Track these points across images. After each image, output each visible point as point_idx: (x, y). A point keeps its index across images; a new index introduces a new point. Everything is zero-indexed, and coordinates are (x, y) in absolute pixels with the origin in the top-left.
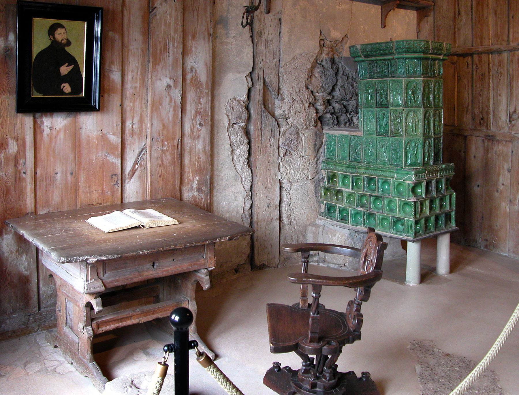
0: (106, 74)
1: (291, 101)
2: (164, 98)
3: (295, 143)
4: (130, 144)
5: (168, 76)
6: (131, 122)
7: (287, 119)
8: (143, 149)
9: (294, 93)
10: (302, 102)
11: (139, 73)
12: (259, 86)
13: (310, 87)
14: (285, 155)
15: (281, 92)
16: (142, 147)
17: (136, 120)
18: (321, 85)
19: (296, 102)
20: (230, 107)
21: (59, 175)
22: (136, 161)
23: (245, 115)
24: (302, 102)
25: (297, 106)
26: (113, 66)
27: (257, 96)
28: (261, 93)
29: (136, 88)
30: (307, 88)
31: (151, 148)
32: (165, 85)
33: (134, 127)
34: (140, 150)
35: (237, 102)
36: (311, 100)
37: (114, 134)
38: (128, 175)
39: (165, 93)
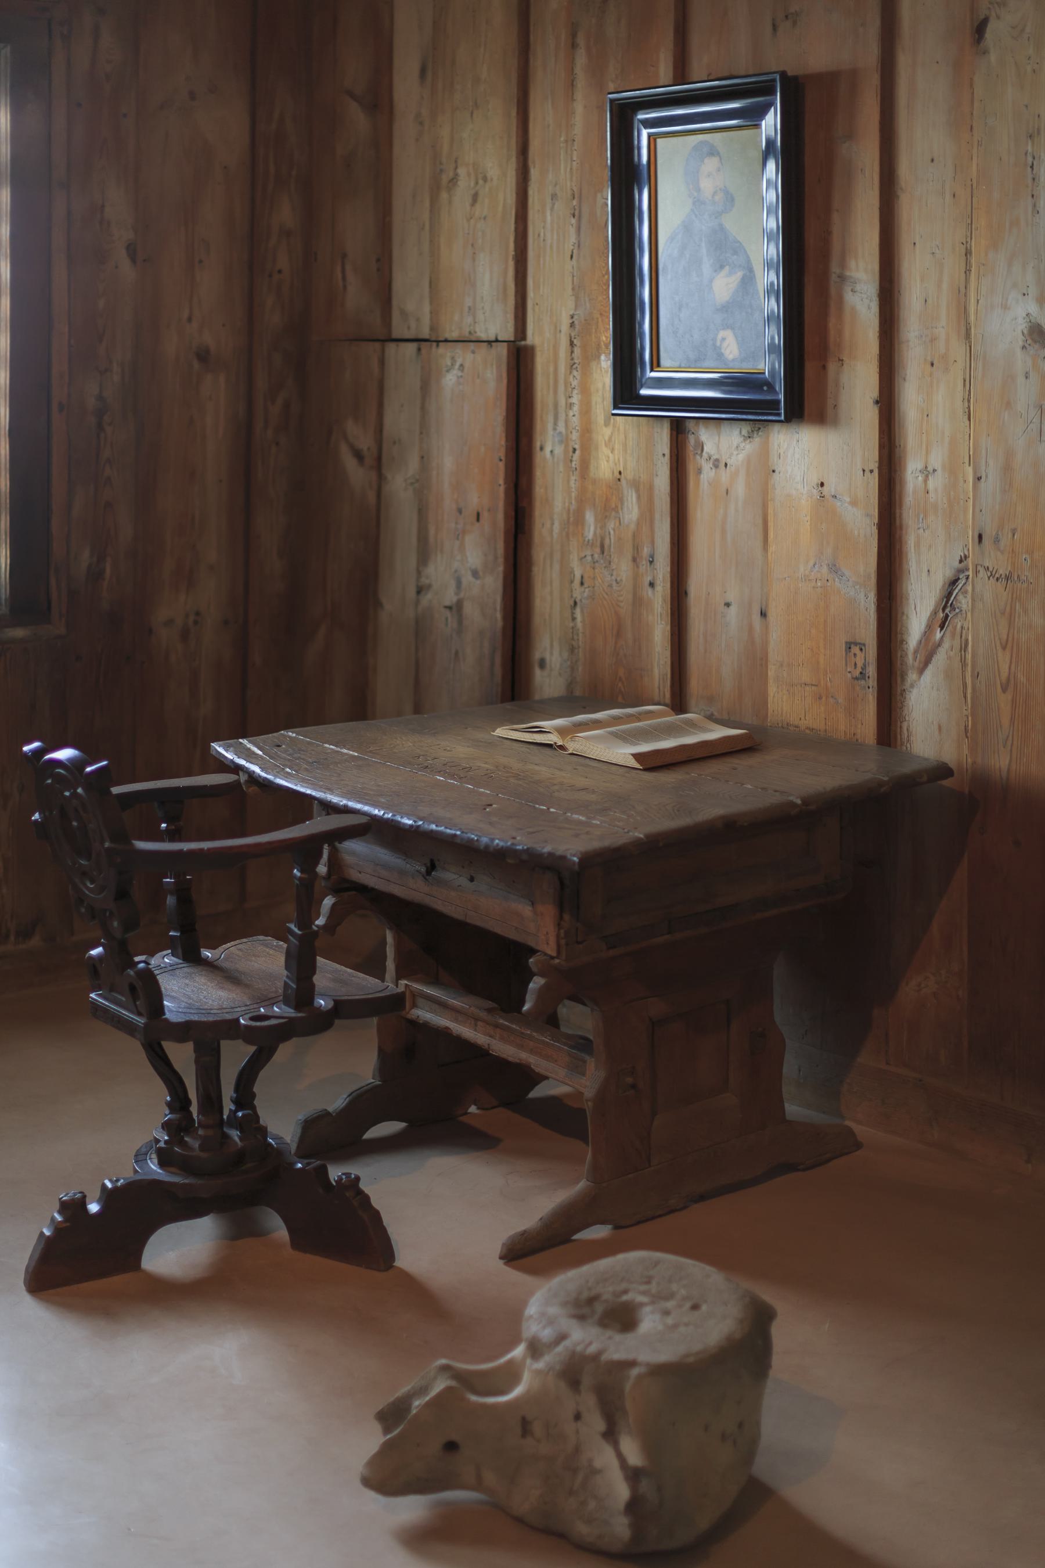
0: (833, 291)
2: (1020, 379)
4: (918, 545)
5: (1033, 291)
6: (920, 466)
8: (960, 571)
11: (945, 286)
16: (956, 564)
17: (937, 459)
21: (733, 609)
22: (935, 613)
26: (852, 264)
29: (933, 340)
31: (977, 572)
32: (1022, 326)
33: (931, 484)
34: (949, 574)
37: (854, 503)
38: (915, 659)
39: (1021, 361)
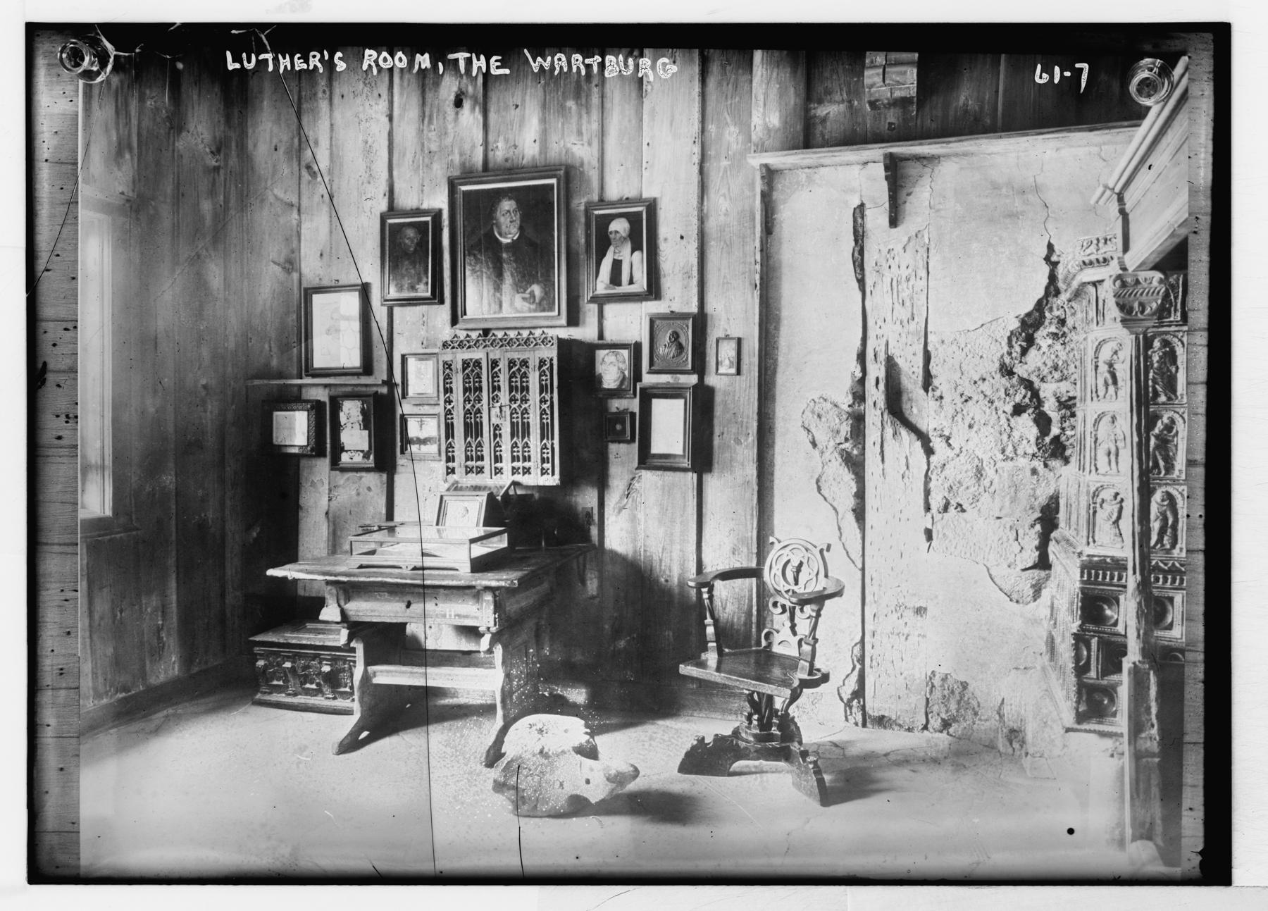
1: (959, 400)
3: (972, 489)
7: (948, 438)
9: (967, 383)
10: (992, 402)
12: (876, 371)
13: (1020, 370)
14: (946, 508)
15: (936, 382)
18: (1050, 364)
19: (970, 403)
20: (813, 412)
23: (846, 428)
24: (992, 402)
25: (976, 410)
27: (876, 395)
28: (882, 386)
30: (1007, 371)
35: (829, 406)
36: (1018, 399)
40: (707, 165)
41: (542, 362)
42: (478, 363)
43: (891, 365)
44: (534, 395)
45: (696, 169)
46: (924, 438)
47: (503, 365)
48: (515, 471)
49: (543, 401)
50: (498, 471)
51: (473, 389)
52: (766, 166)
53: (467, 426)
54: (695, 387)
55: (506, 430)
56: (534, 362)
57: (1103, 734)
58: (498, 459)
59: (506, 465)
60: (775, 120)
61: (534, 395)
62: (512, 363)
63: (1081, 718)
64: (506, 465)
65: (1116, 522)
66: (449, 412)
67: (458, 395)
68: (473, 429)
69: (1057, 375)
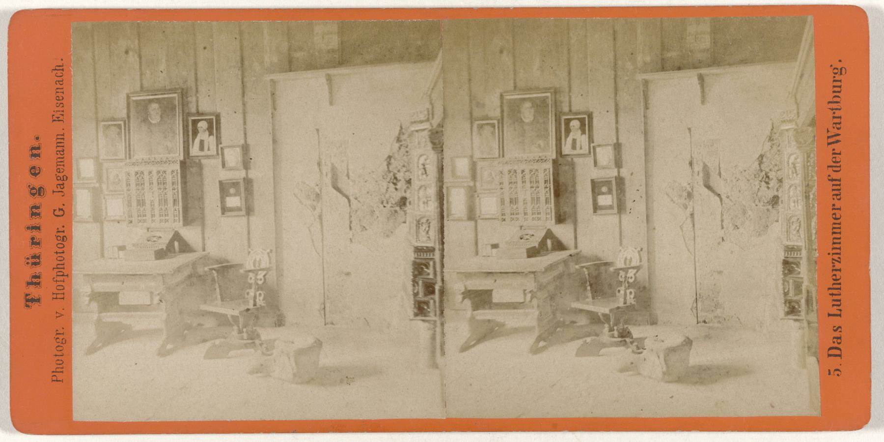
40: (245, 79)
41: (173, 172)
42: (142, 173)
43: (334, 169)
44: (169, 186)
45: (240, 82)
46: (347, 197)
47: (154, 173)
48: (161, 221)
49: (174, 189)
50: (153, 221)
51: (140, 184)
52: (272, 80)
53: (138, 201)
54: (244, 179)
55: (156, 204)
56: (169, 172)
57: (423, 321)
58: (153, 216)
59: (157, 218)
60: (275, 59)
61: (169, 186)
62: (159, 172)
63: (416, 315)
64: (157, 218)
65: (427, 232)
66: (129, 195)
67: (133, 186)
68: (141, 203)
69: (404, 169)
